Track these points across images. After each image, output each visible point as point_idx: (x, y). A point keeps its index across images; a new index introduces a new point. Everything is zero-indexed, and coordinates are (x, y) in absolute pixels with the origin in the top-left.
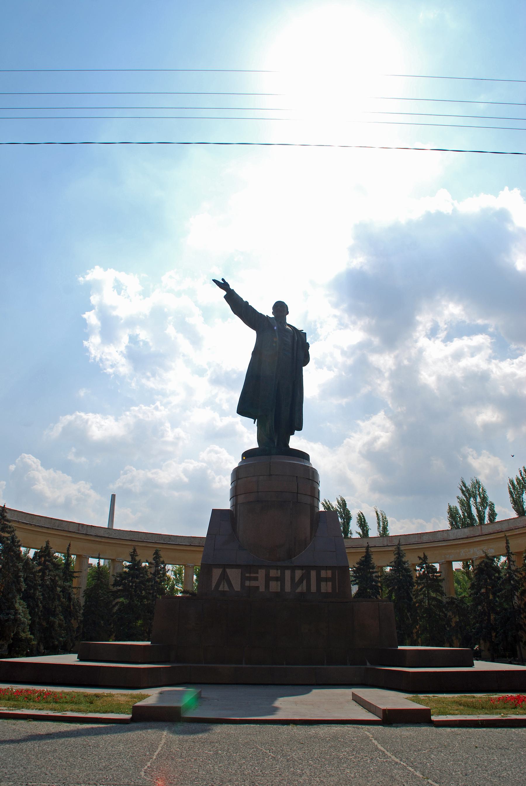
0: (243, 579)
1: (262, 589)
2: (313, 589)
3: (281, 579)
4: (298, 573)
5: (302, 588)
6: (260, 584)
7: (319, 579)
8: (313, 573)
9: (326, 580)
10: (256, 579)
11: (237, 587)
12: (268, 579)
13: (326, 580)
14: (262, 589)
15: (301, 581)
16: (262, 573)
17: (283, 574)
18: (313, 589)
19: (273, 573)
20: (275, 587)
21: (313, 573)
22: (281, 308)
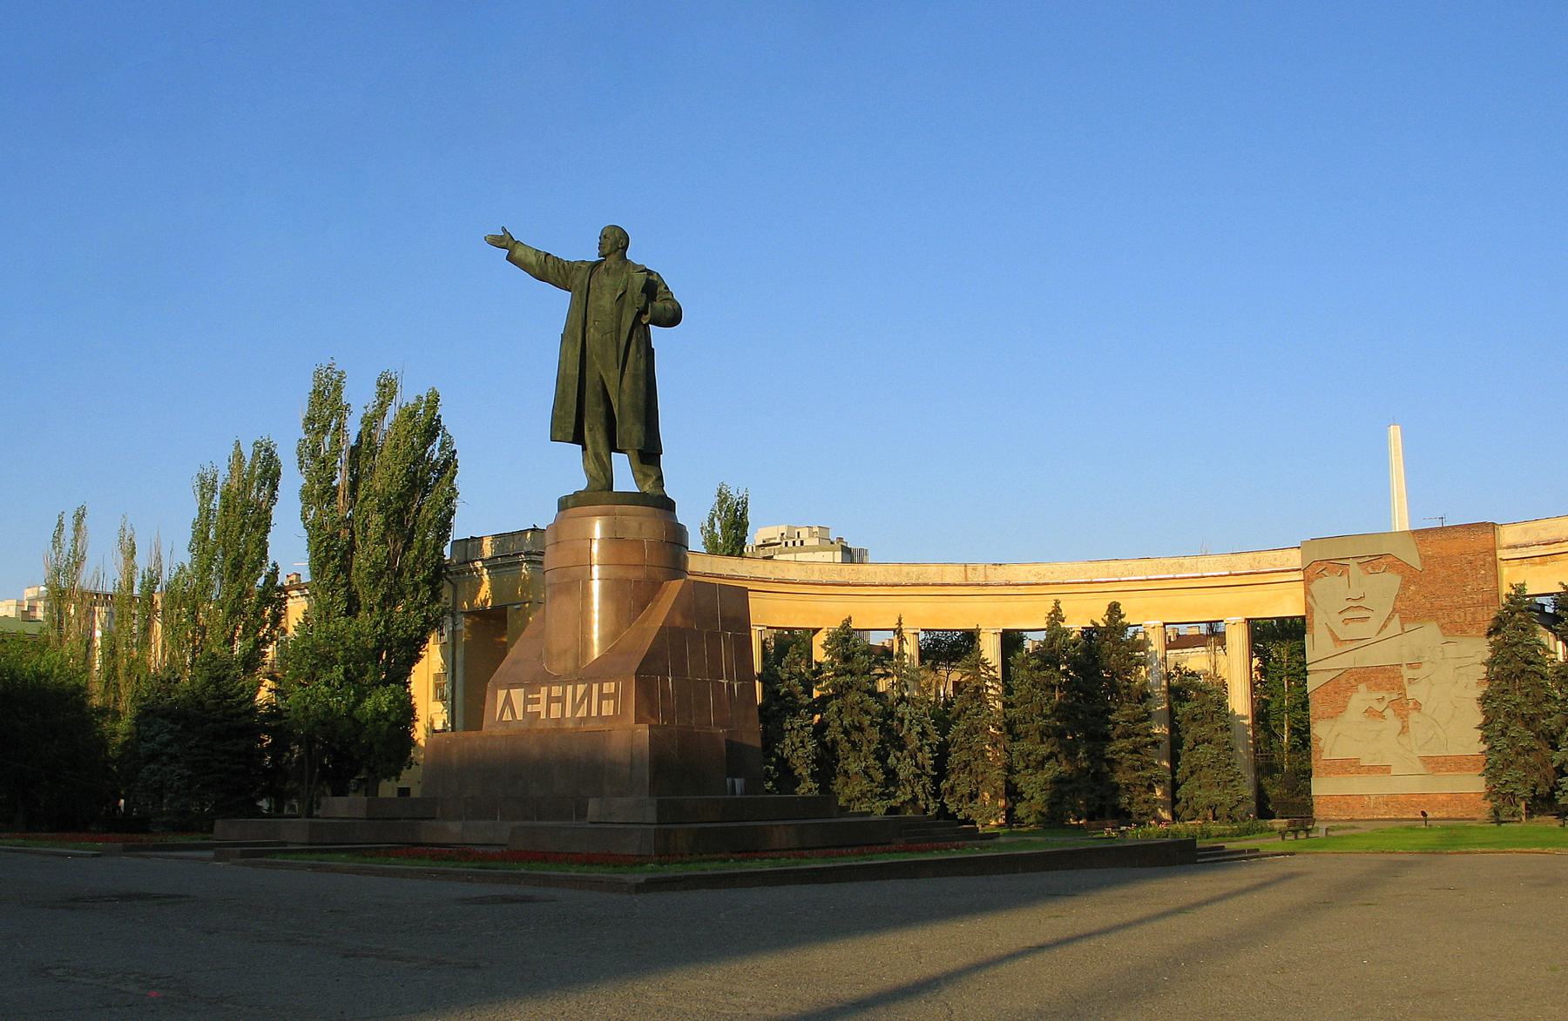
0: (527, 702)
1: (543, 716)
2: (594, 714)
3: (561, 700)
4: (581, 688)
5: (582, 713)
6: (541, 708)
7: (602, 697)
8: (595, 687)
9: (608, 697)
10: (537, 701)
11: (520, 717)
12: (550, 700)
13: (608, 697)
14: (543, 716)
15: (582, 699)
16: (544, 690)
17: (564, 691)
18: (594, 713)
19: (556, 691)
20: (556, 710)
21: (595, 687)
22: (615, 242)
